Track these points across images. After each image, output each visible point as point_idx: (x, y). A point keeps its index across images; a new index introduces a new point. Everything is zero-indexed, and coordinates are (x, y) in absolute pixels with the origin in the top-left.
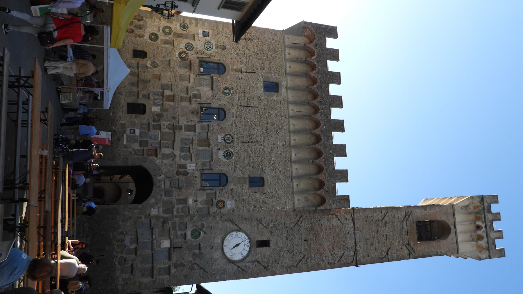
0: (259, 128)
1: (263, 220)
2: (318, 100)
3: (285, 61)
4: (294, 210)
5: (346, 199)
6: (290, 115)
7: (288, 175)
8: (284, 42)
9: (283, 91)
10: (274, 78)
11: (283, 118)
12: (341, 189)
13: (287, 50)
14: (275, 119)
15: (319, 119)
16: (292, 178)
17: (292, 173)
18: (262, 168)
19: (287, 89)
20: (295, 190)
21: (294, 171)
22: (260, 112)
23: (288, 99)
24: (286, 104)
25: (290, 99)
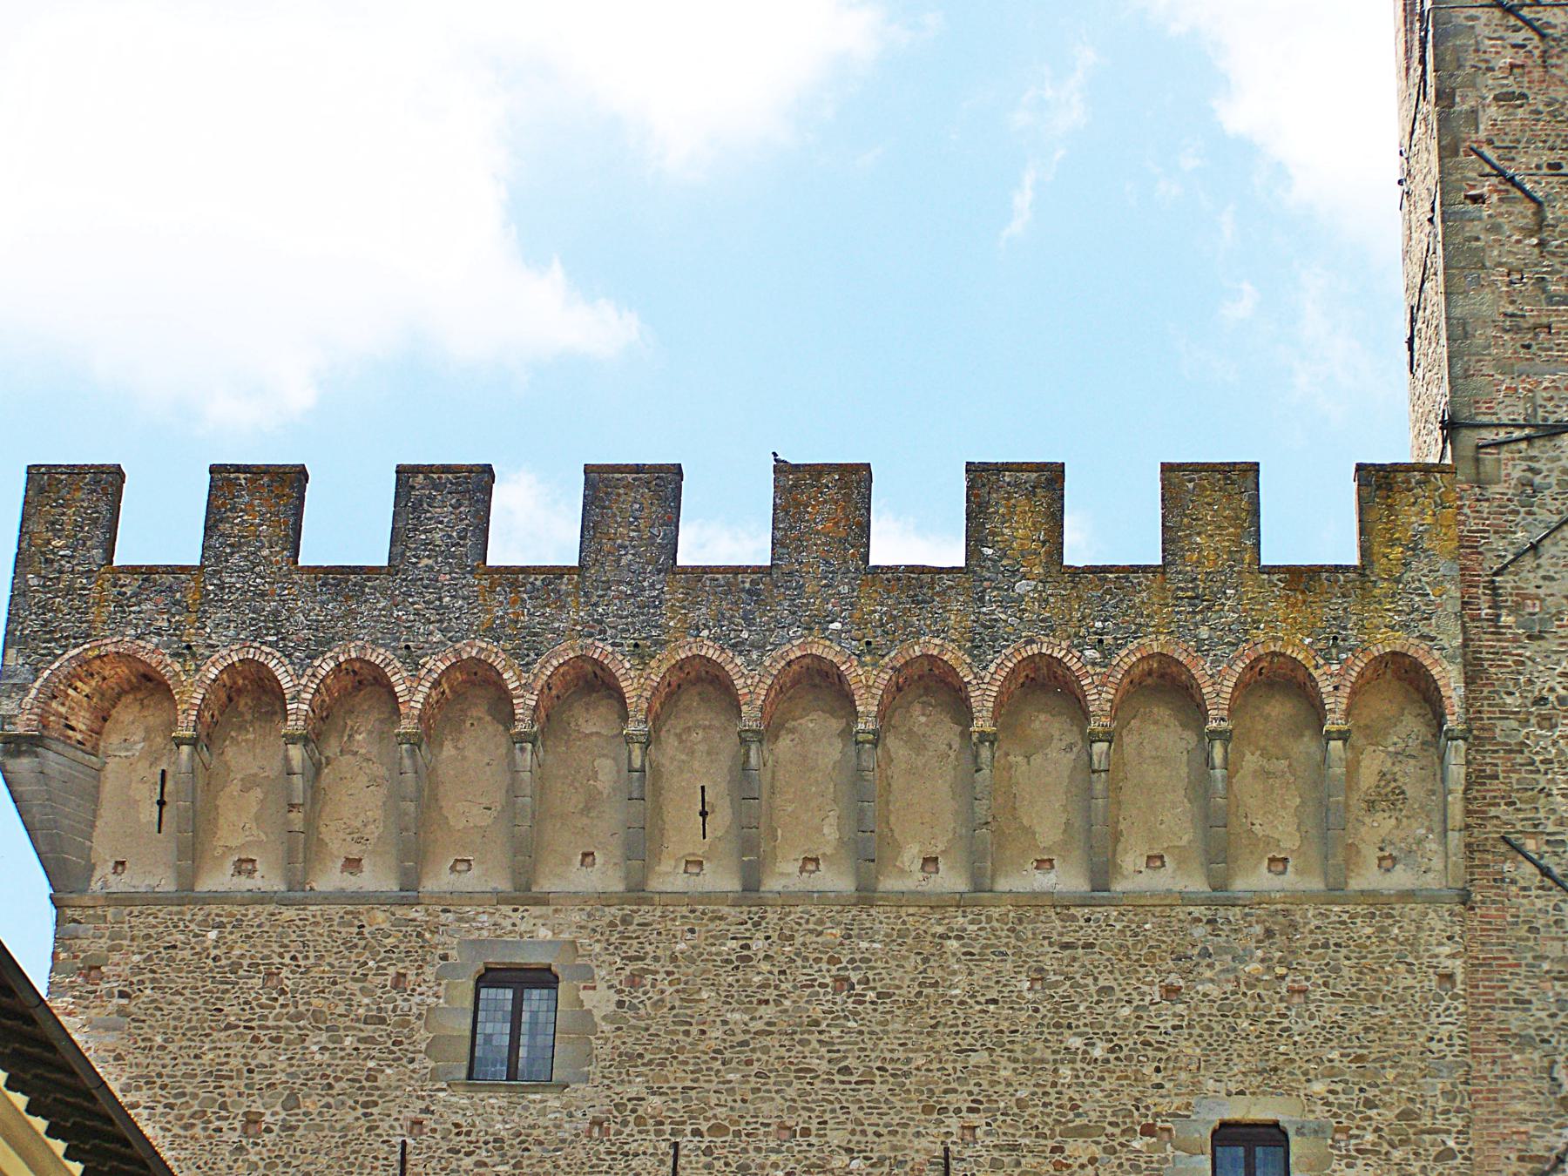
0: (836, 1138)
1: (1538, 1148)
2: (624, 670)
3: (303, 904)
4: (1465, 899)
5: (1377, 483)
6: (731, 884)
7: (1199, 931)
8: (151, 899)
9: (544, 933)
10: (444, 1001)
11: (758, 945)
12: (1310, 524)
13: (218, 879)
14: (767, 1012)
15: (773, 663)
16: (1220, 896)
17: (1187, 899)
18: (1148, 1130)
19: (524, 895)
20: (1316, 884)
21: (1167, 880)
22: (718, 1129)
23: (604, 899)
24: (647, 913)
25: (605, 877)
